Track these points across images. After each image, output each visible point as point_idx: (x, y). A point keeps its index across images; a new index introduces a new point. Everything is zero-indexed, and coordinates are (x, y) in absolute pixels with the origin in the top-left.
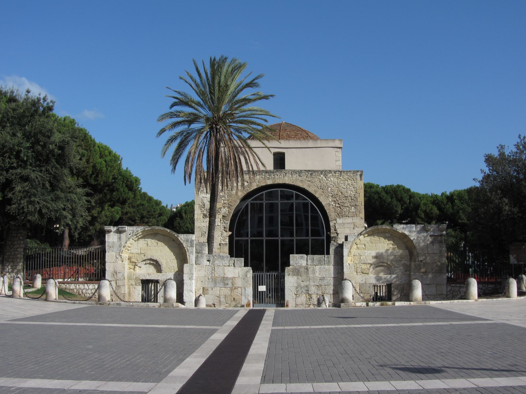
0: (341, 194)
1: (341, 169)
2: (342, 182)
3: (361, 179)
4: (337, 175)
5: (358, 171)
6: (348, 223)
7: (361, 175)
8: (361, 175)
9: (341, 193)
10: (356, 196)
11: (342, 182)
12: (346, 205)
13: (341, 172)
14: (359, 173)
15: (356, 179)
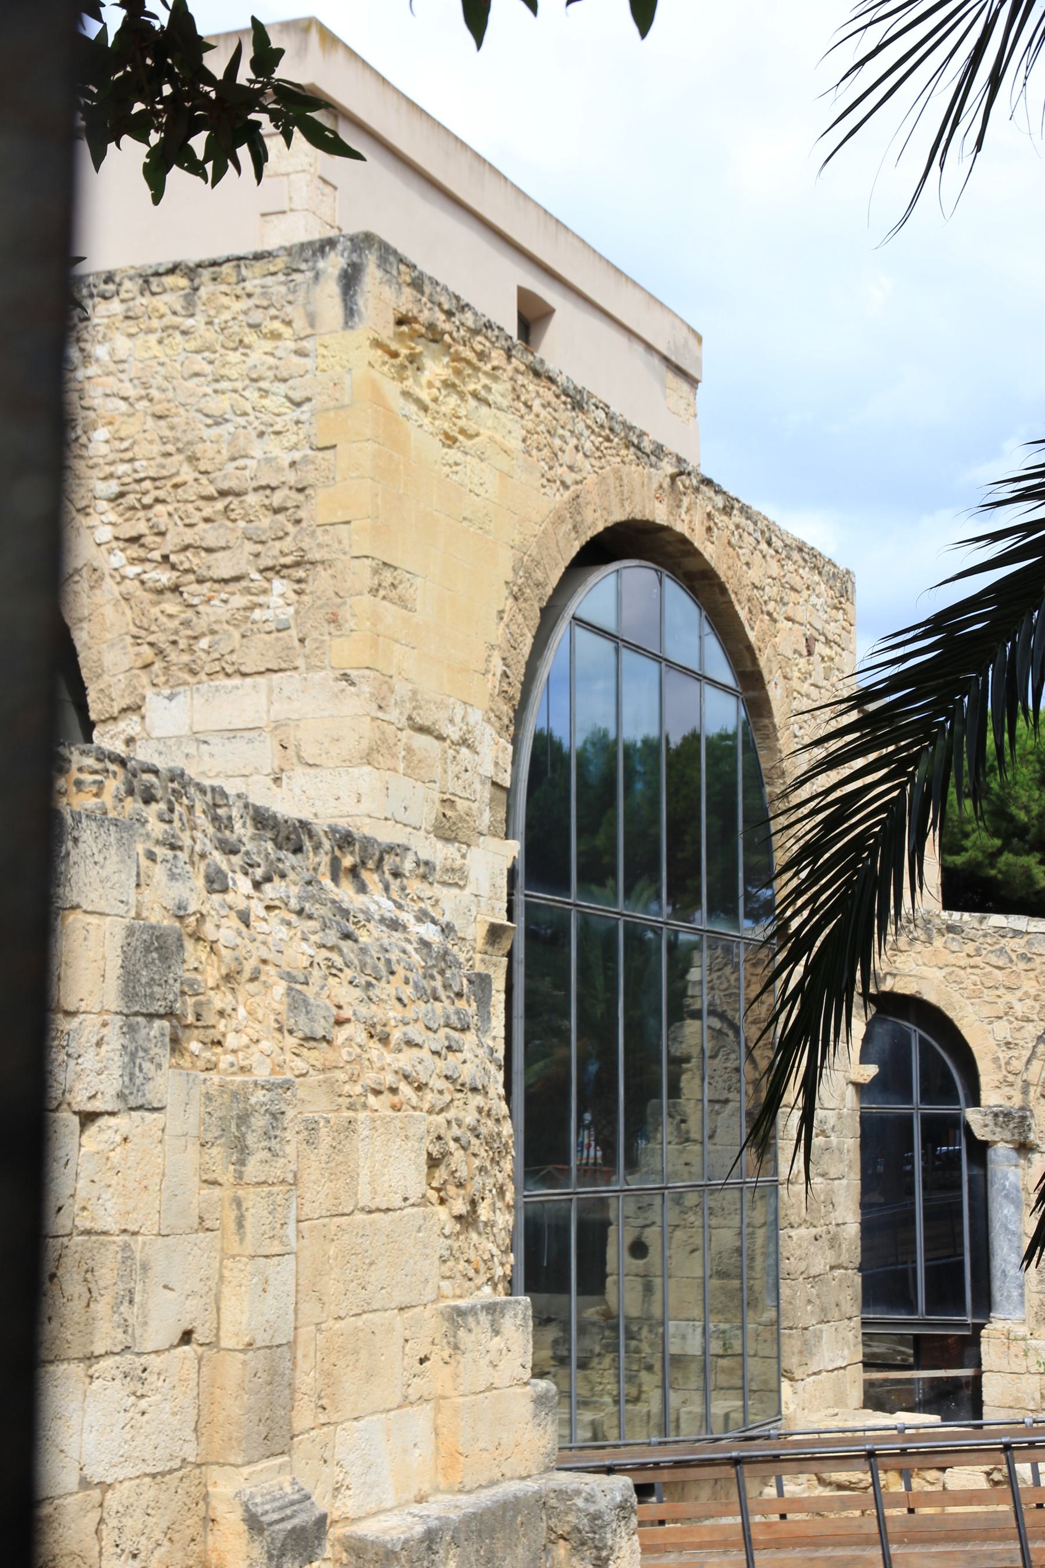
0: (187, 473)
1: (192, 256)
2: (199, 363)
3: (350, 312)
4: (160, 303)
5: (326, 245)
6: (232, 733)
7: (350, 280)
8: (350, 280)
9: (193, 459)
10: (309, 476)
11: (199, 363)
12: (223, 566)
13: (191, 271)
14: (334, 264)
15: (312, 320)
